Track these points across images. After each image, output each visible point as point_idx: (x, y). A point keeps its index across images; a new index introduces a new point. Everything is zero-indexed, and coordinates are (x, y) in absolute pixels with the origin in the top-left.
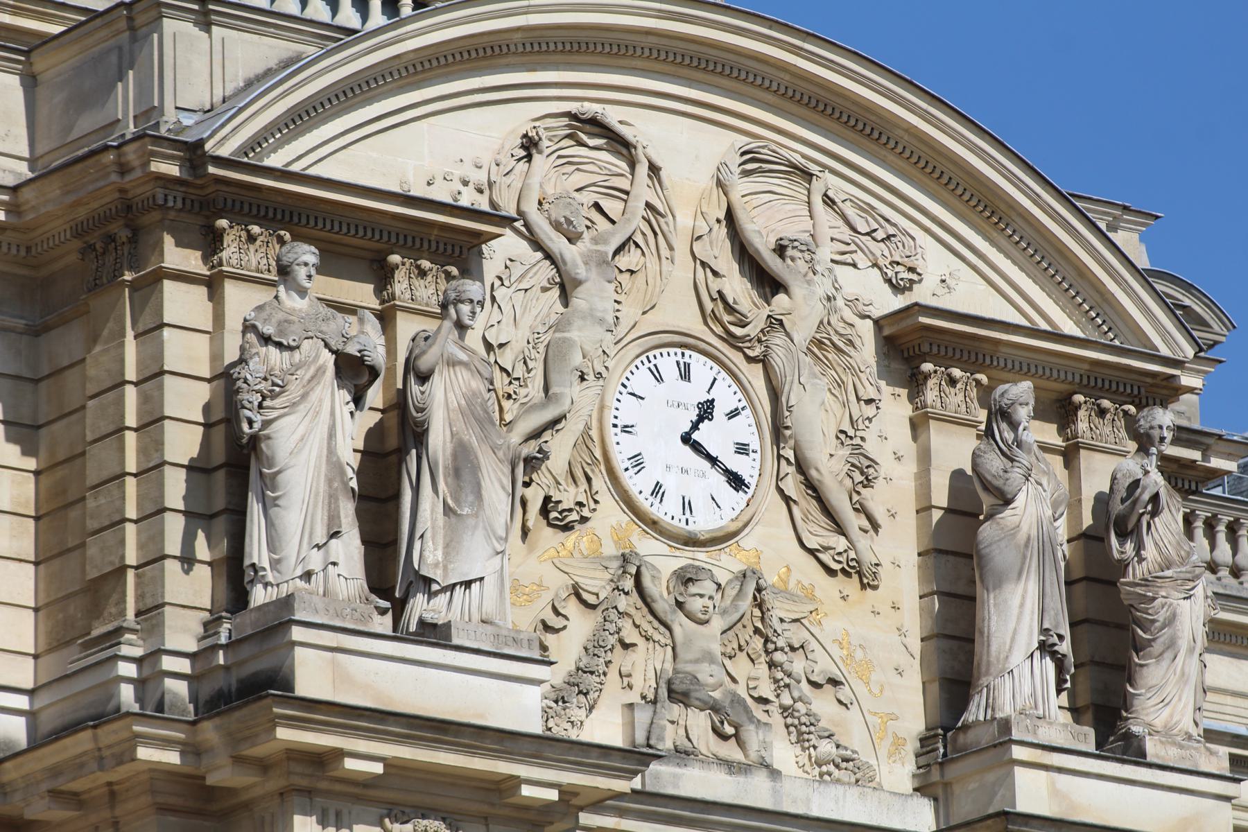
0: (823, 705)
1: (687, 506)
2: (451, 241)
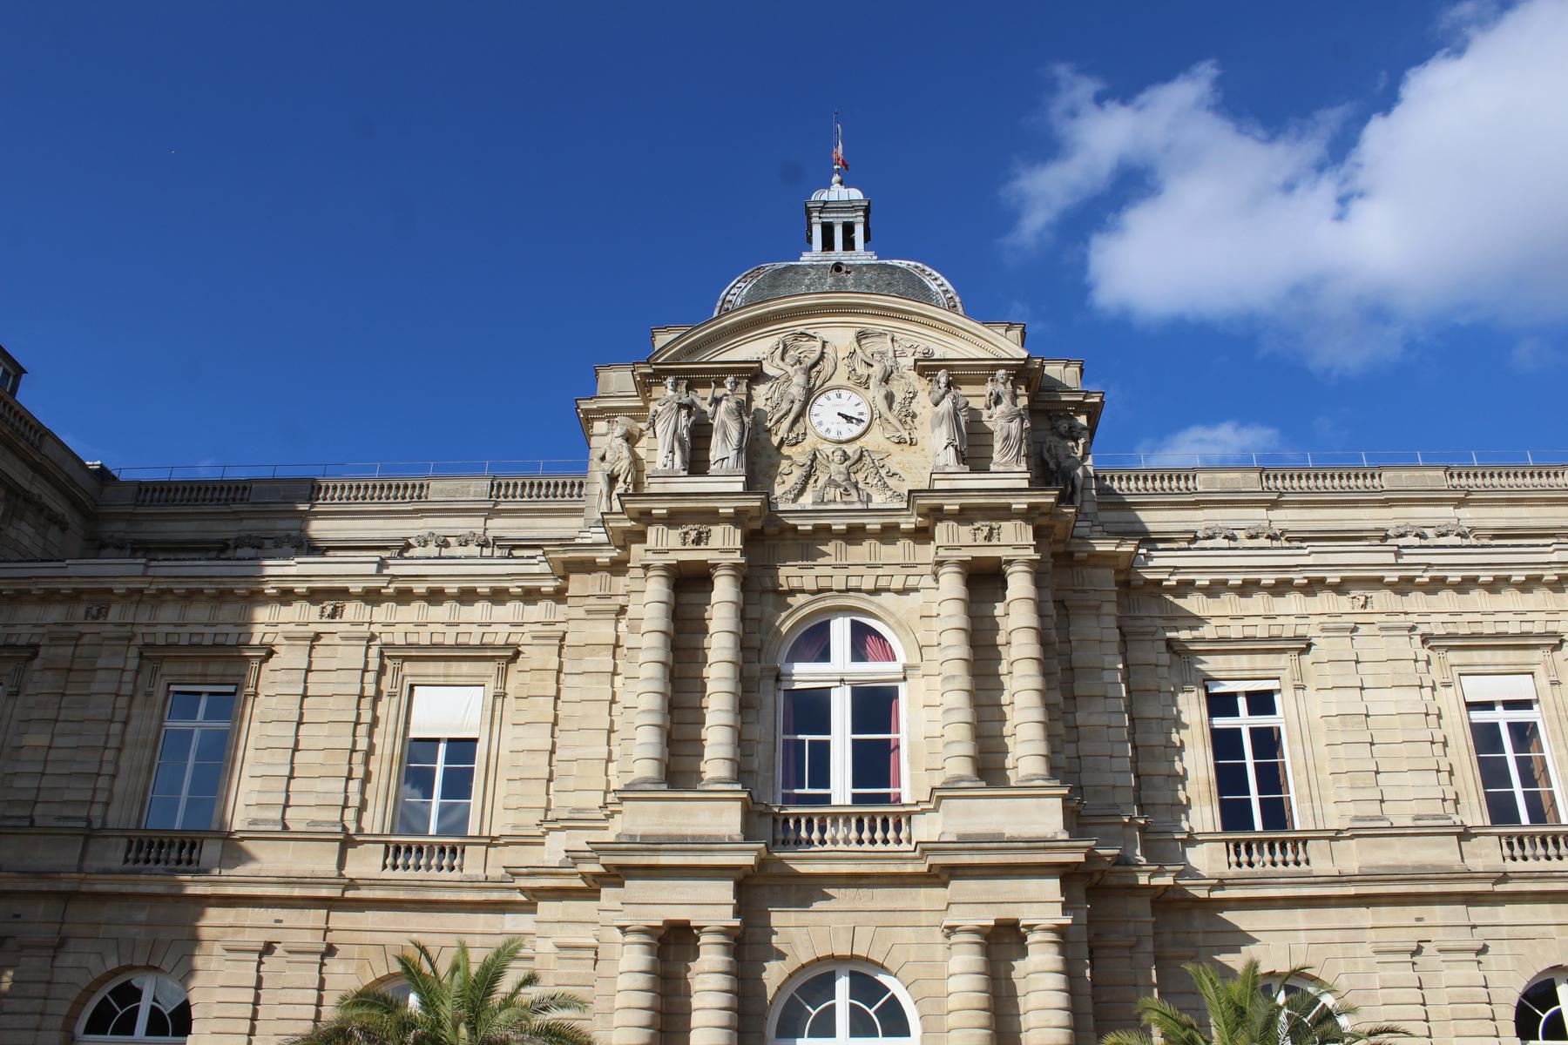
0: (891, 482)
1: (839, 433)
2: (753, 374)
